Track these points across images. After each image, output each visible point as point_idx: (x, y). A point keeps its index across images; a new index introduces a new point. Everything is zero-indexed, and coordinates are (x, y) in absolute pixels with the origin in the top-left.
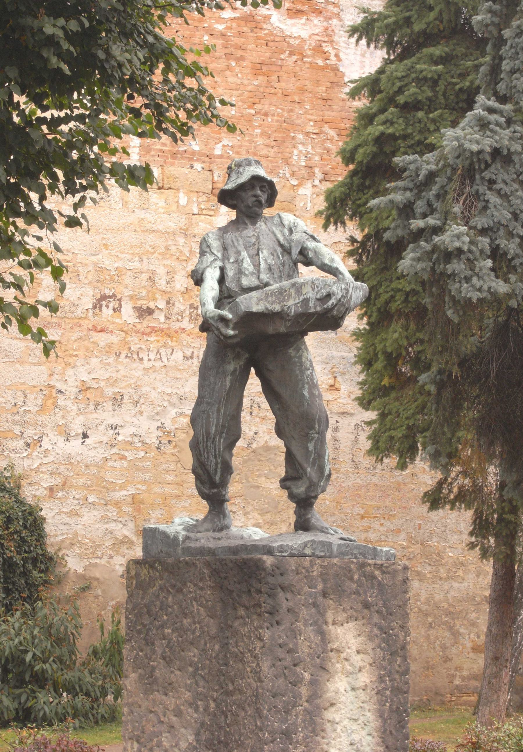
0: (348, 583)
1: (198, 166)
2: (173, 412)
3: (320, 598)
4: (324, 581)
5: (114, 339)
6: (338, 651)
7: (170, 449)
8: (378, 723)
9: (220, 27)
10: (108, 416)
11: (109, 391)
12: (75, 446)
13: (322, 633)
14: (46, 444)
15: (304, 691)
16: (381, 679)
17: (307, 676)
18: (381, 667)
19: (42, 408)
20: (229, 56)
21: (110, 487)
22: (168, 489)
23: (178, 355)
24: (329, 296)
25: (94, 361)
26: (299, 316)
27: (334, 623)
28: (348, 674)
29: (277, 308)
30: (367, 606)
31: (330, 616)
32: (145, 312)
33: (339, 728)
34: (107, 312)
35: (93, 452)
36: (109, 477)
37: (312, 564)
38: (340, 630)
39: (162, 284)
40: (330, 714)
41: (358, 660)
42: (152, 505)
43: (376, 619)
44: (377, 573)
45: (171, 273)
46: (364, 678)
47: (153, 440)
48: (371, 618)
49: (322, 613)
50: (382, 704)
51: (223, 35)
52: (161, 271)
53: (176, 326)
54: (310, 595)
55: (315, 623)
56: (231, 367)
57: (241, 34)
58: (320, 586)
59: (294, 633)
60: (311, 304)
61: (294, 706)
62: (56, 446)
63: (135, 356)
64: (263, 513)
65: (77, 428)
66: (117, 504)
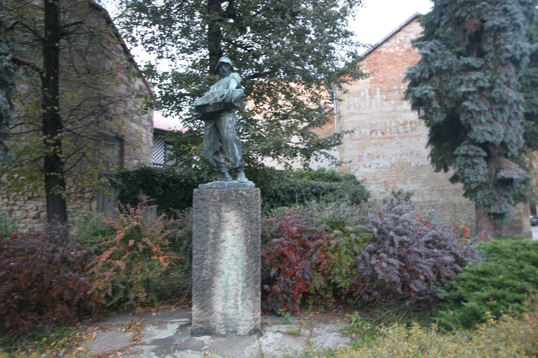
0: (231, 197)
1: (396, 93)
2: (394, 158)
3: (218, 203)
4: (220, 197)
5: (376, 141)
6: (226, 222)
7: (394, 168)
8: (245, 248)
9: (400, 54)
10: (376, 161)
11: (376, 155)
12: (368, 170)
13: (219, 215)
14: (360, 170)
15: (211, 236)
16: (246, 231)
17: (212, 231)
18: (246, 227)
19: (358, 161)
20: (403, 61)
21: (378, 179)
22: (394, 179)
23: (394, 143)
24: (223, 95)
25: (371, 148)
26: (214, 104)
27: (225, 212)
28: (232, 230)
29: (206, 103)
30: (239, 205)
31: (223, 209)
32: (383, 133)
33: (227, 250)
34: (374, 134)
35: (372, 170)
36: (377, 176)
37: (214, 191)
38: (228, 214)
39: (388, 125)
40: (223, 244)
41: (236, 225)
42: (390, 183)
43: (244, 209)
44: (244, 193)
45: (391, 122)
46: (239, 231)
47: (389, 166)
48: (242, 209)
49: (219, 208)
50: (246, 241)
51: (401, 56)
52: (388, 122)
53: (393, 136)
54: (214, 202)
55: (217, 212)
56: (208, 127)
57: (406, 55)
58: (218, 199)
59: (207, 216)
60: (218, 99)
61: (206, 241)
62: (362, 170)
63: (382, 145)
64: (422, 183)
65: (368, 164)
66: (380, 183)
